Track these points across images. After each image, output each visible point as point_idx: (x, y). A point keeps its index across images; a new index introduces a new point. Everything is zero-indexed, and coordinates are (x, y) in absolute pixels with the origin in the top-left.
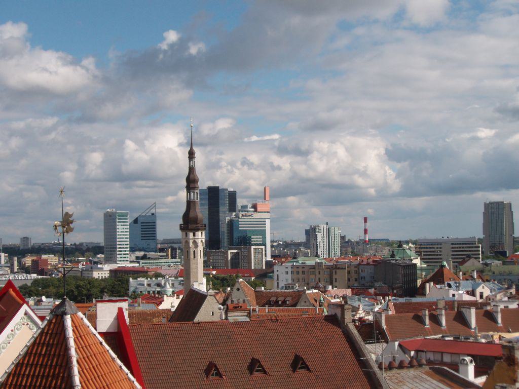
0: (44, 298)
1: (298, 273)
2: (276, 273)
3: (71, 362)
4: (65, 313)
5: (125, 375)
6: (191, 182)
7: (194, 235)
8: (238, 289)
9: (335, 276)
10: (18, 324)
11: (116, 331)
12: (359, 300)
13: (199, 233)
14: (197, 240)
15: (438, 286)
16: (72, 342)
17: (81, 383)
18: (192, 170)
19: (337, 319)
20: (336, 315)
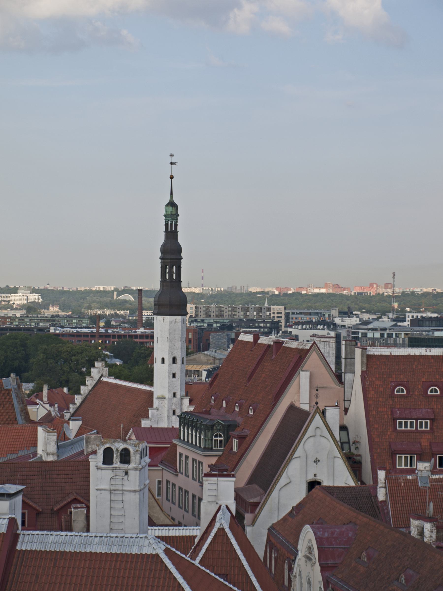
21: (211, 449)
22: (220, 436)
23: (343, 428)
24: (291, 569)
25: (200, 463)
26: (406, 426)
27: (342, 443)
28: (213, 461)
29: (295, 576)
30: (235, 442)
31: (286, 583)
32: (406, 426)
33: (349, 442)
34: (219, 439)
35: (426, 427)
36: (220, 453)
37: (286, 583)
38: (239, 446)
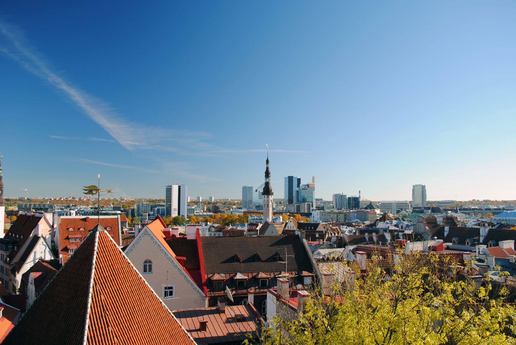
0: (208, 223)
1: (322, 215)
2: (313, 215)
3: (94, 253)
4: (97, 231)
5: (126, 260)
6: (267, 174)
7: (268, 197)
8: (291, 222)
9: (339, 217)
10: (142, 234)
11: (196, 239)
12: (346, 228)
13: (270, 196)
14: (269, 199)
15: (382, 223)
16: (96, 244)
17: (96, 263)
18: (267, 168)
19: (299, 237)
20: (298, 235)
21: (8, 250)
22: (11, 246)
23: (53, 241)
24: (27, 287)
25: (4, 255)
26: (73, 240)
27: (52, 246)
28: (8, 254)
29: (28, 290)
30: (16, 247)
31: (26, 291)
32: (73, 240)
33: (55, 246)
34: (10, 247)
35: (79, 240)
36: (11, 251)
37: (26, 291)
38: (17, 248)
